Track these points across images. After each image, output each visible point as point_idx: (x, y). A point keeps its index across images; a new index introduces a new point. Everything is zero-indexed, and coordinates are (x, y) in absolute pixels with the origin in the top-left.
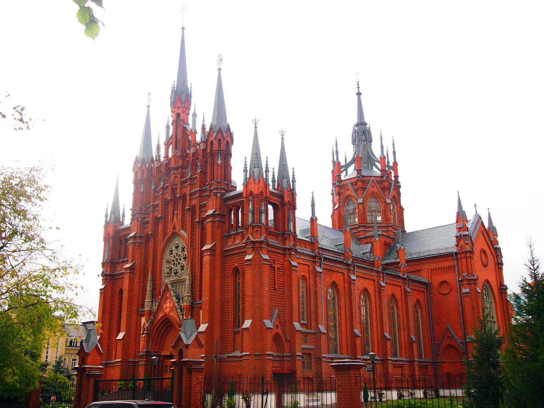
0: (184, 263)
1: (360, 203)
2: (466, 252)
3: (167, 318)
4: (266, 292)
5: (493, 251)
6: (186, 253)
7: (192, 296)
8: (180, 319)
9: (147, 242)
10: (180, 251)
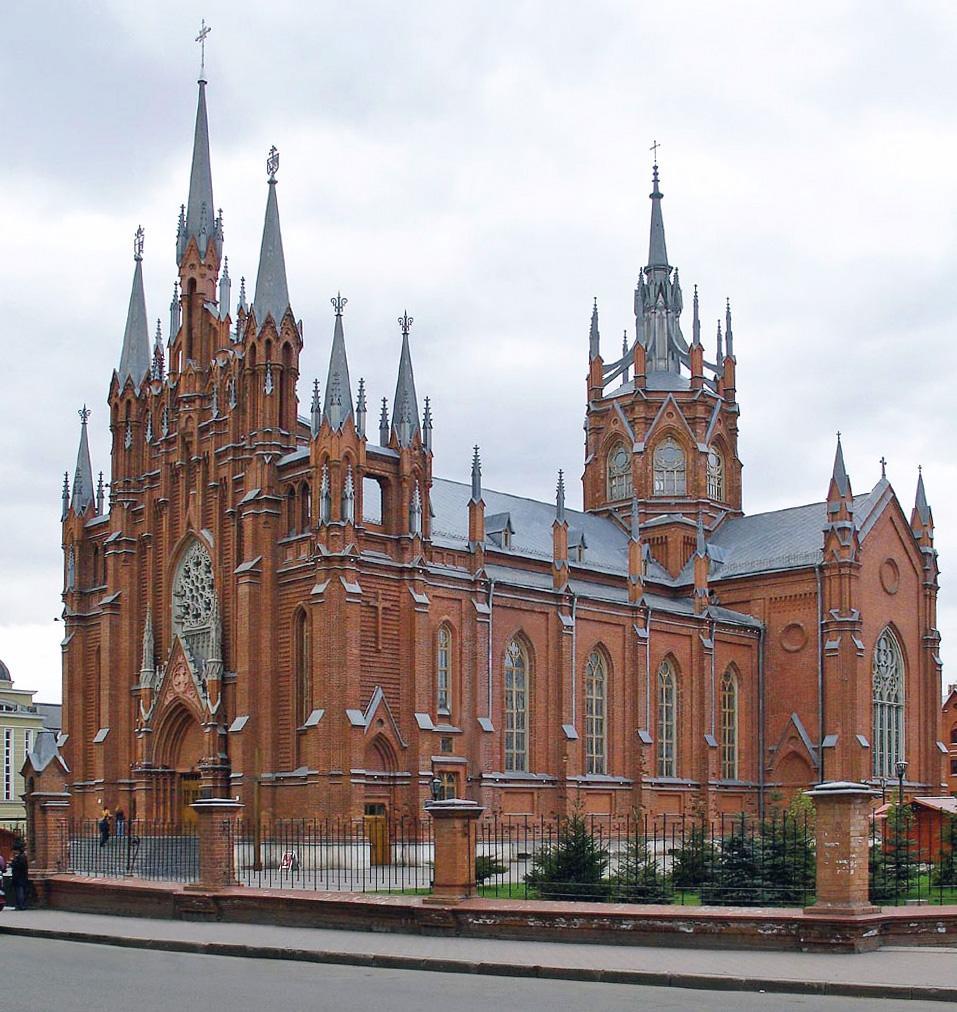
0: (210, 596)
2: (842, 565)
3: (181, 705)
5: (915, 560)
6: (212, 576)
9: (143, 552)
10: (202, 572)
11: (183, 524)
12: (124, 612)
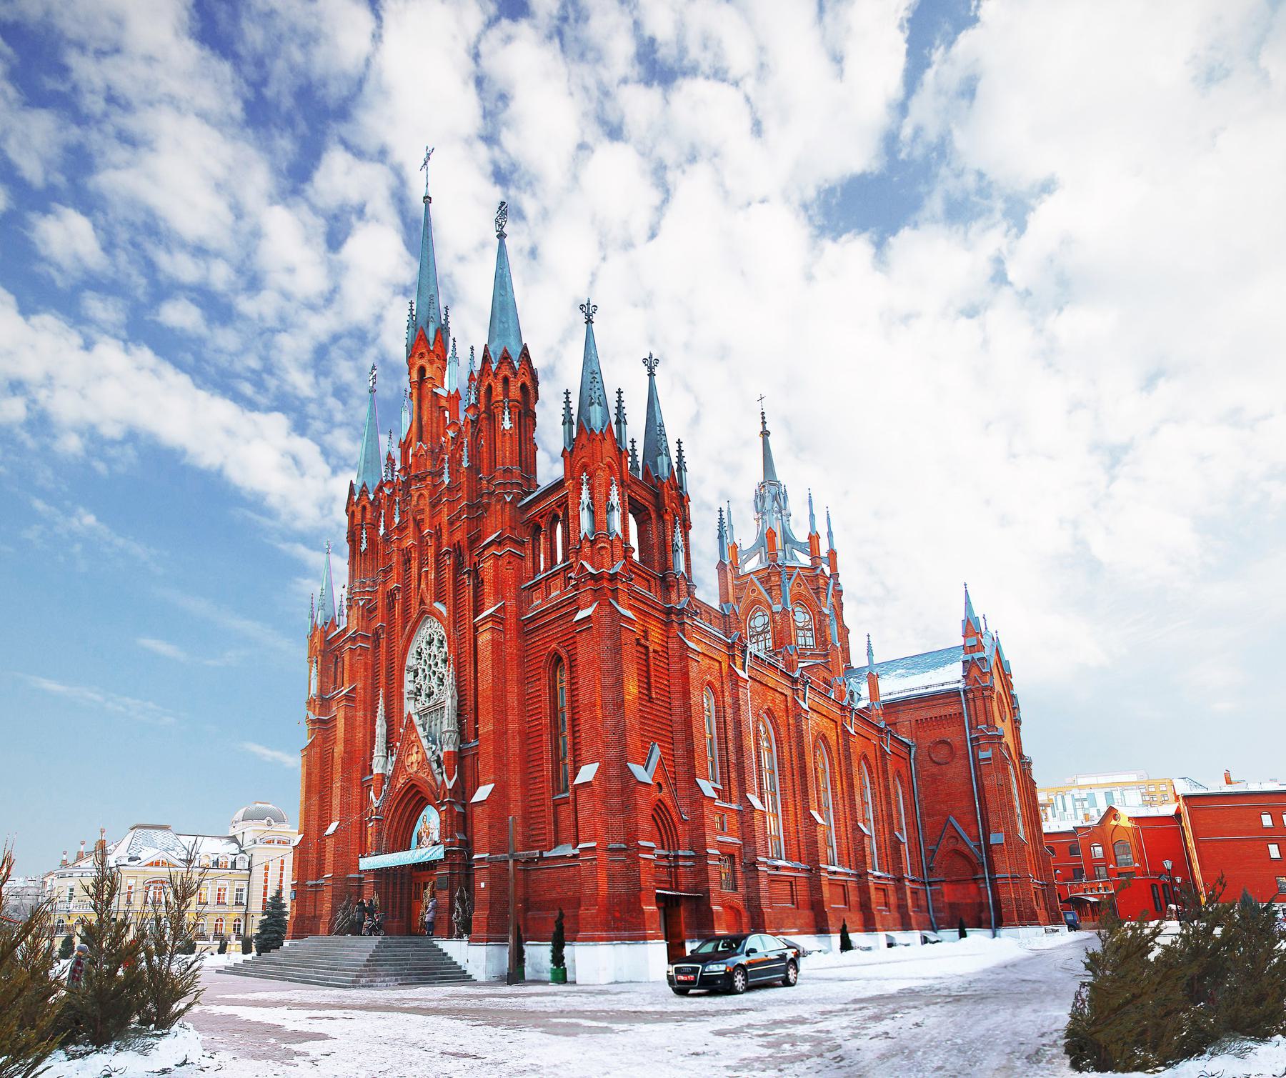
4: (631, 698)
7: (459, 733)
11: (415, 602)
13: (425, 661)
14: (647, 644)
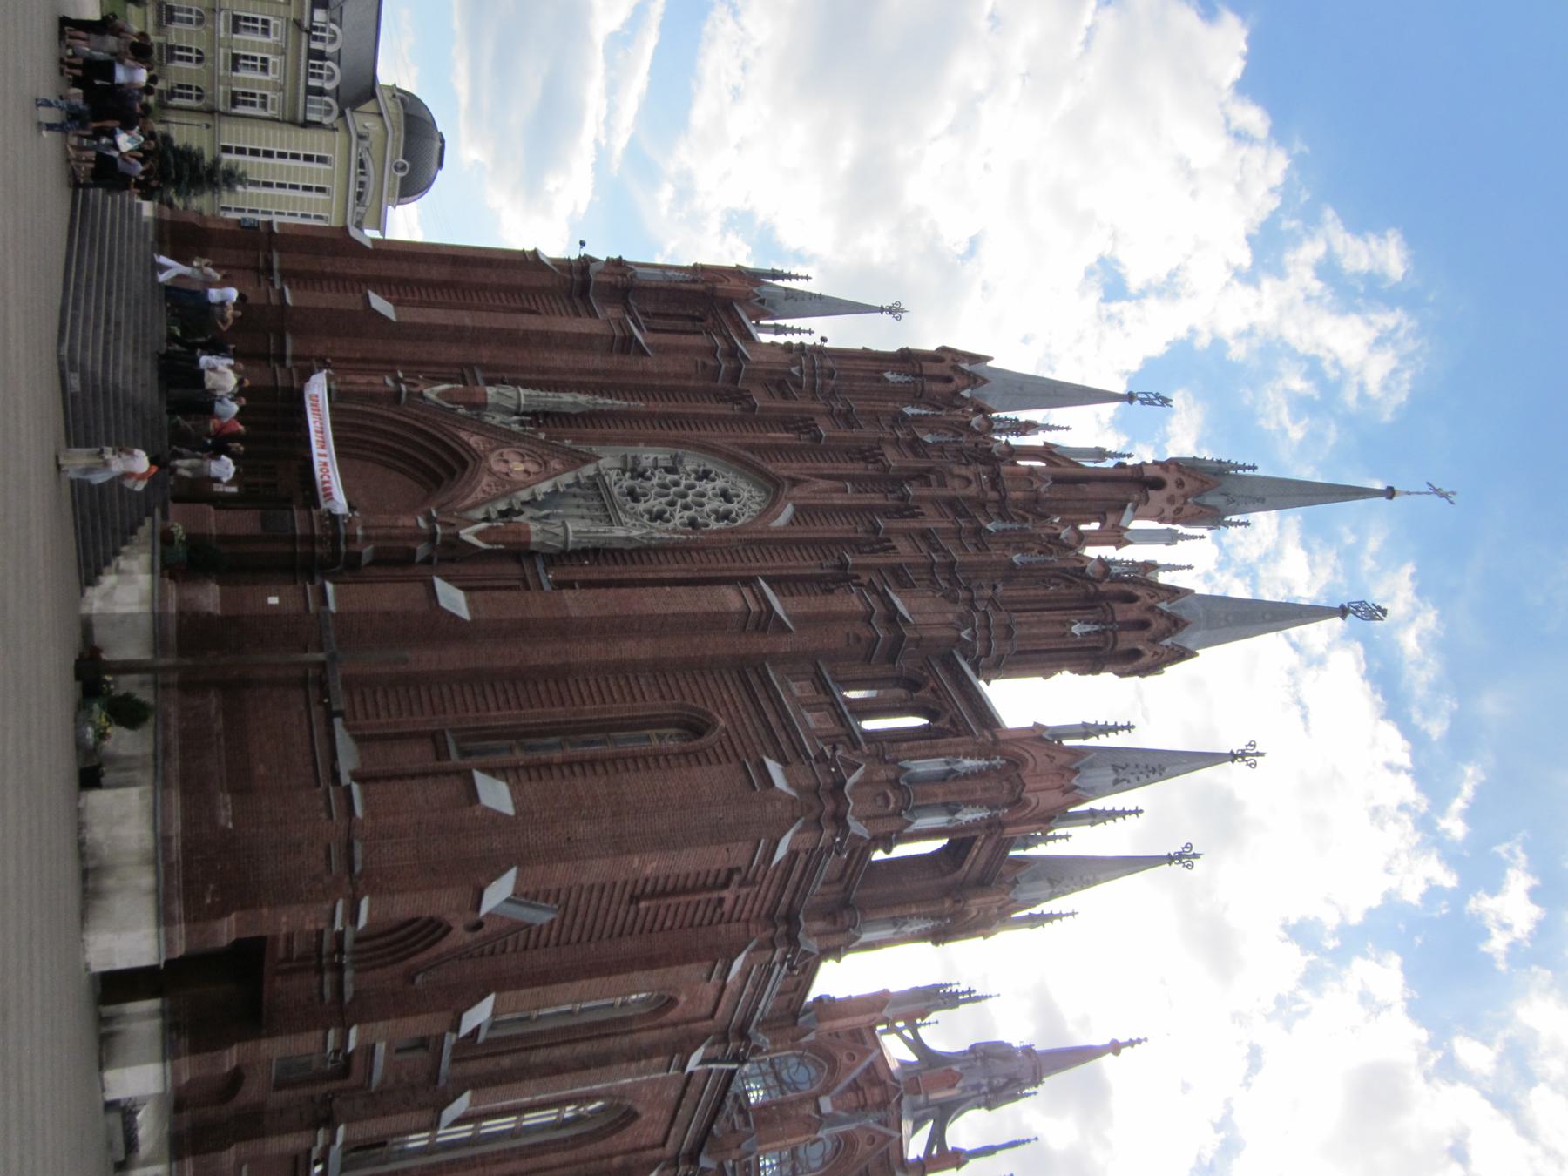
0: (676, 522)
1: (818, 1109)
3: (464, 464)
4: (636, 864)
6: (714, 525)
8: (468, 509)
9: (721, 397)
12: (613, 362)
13: (692, 487)
14: (733, 887)
